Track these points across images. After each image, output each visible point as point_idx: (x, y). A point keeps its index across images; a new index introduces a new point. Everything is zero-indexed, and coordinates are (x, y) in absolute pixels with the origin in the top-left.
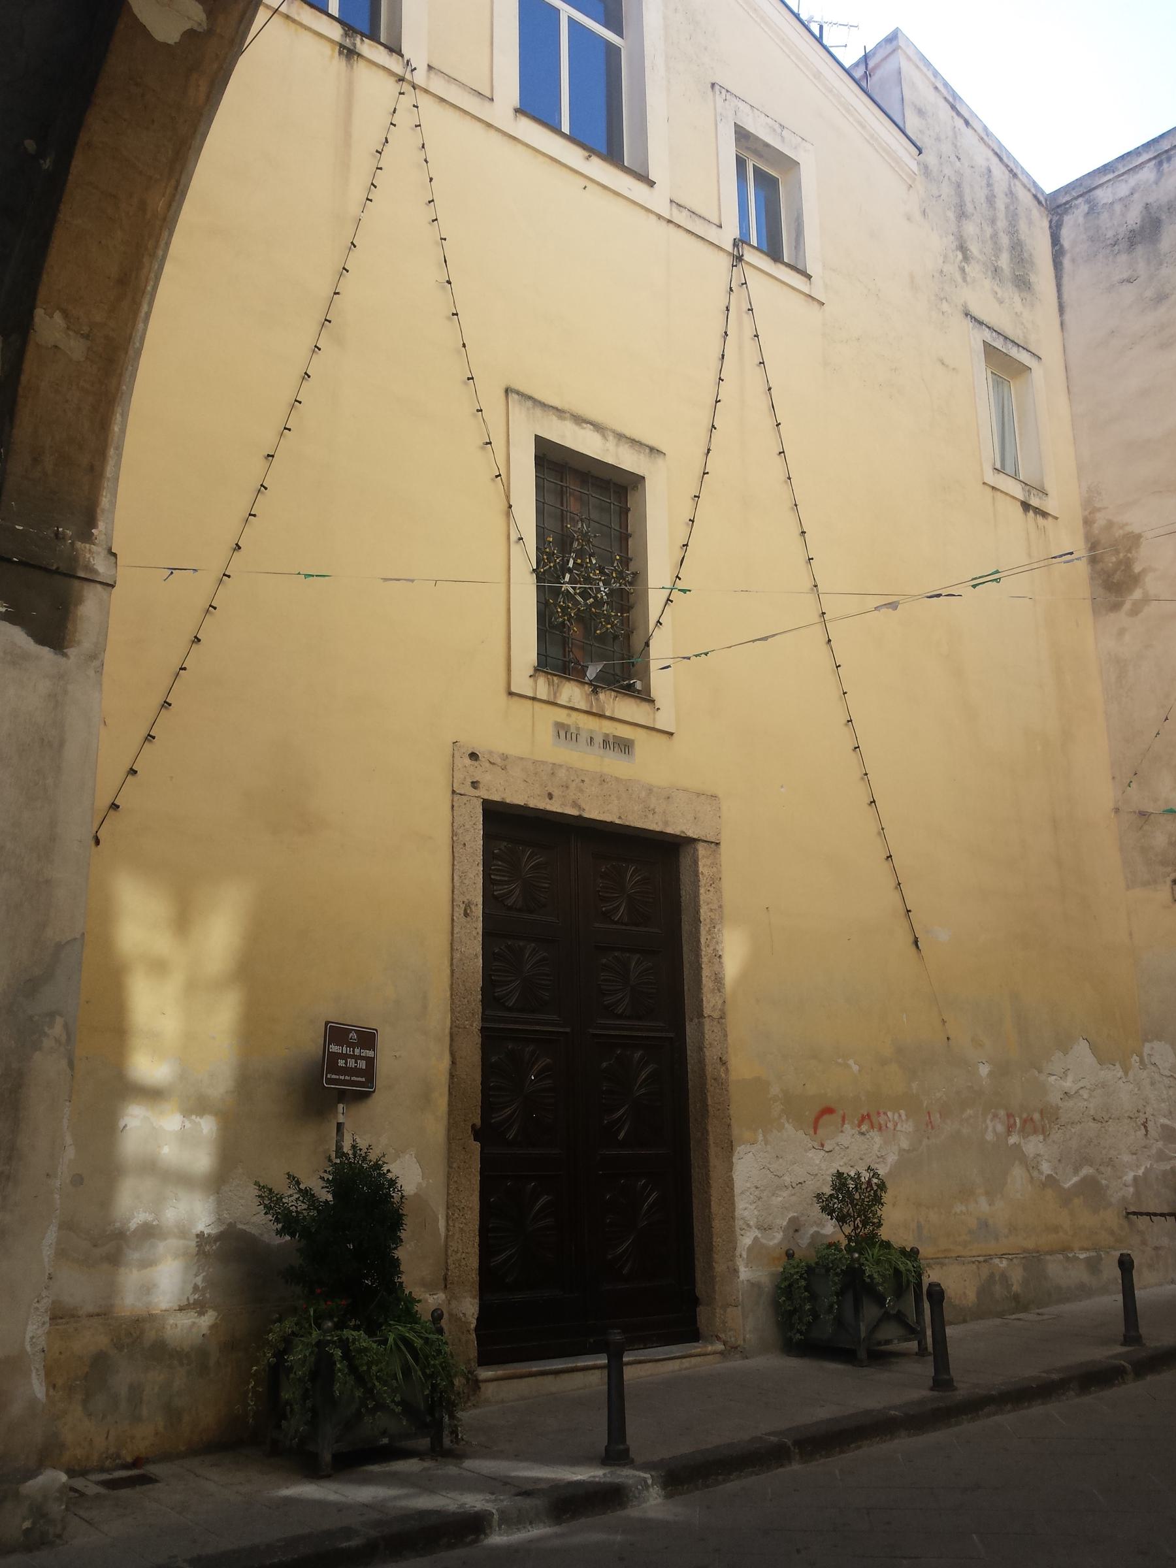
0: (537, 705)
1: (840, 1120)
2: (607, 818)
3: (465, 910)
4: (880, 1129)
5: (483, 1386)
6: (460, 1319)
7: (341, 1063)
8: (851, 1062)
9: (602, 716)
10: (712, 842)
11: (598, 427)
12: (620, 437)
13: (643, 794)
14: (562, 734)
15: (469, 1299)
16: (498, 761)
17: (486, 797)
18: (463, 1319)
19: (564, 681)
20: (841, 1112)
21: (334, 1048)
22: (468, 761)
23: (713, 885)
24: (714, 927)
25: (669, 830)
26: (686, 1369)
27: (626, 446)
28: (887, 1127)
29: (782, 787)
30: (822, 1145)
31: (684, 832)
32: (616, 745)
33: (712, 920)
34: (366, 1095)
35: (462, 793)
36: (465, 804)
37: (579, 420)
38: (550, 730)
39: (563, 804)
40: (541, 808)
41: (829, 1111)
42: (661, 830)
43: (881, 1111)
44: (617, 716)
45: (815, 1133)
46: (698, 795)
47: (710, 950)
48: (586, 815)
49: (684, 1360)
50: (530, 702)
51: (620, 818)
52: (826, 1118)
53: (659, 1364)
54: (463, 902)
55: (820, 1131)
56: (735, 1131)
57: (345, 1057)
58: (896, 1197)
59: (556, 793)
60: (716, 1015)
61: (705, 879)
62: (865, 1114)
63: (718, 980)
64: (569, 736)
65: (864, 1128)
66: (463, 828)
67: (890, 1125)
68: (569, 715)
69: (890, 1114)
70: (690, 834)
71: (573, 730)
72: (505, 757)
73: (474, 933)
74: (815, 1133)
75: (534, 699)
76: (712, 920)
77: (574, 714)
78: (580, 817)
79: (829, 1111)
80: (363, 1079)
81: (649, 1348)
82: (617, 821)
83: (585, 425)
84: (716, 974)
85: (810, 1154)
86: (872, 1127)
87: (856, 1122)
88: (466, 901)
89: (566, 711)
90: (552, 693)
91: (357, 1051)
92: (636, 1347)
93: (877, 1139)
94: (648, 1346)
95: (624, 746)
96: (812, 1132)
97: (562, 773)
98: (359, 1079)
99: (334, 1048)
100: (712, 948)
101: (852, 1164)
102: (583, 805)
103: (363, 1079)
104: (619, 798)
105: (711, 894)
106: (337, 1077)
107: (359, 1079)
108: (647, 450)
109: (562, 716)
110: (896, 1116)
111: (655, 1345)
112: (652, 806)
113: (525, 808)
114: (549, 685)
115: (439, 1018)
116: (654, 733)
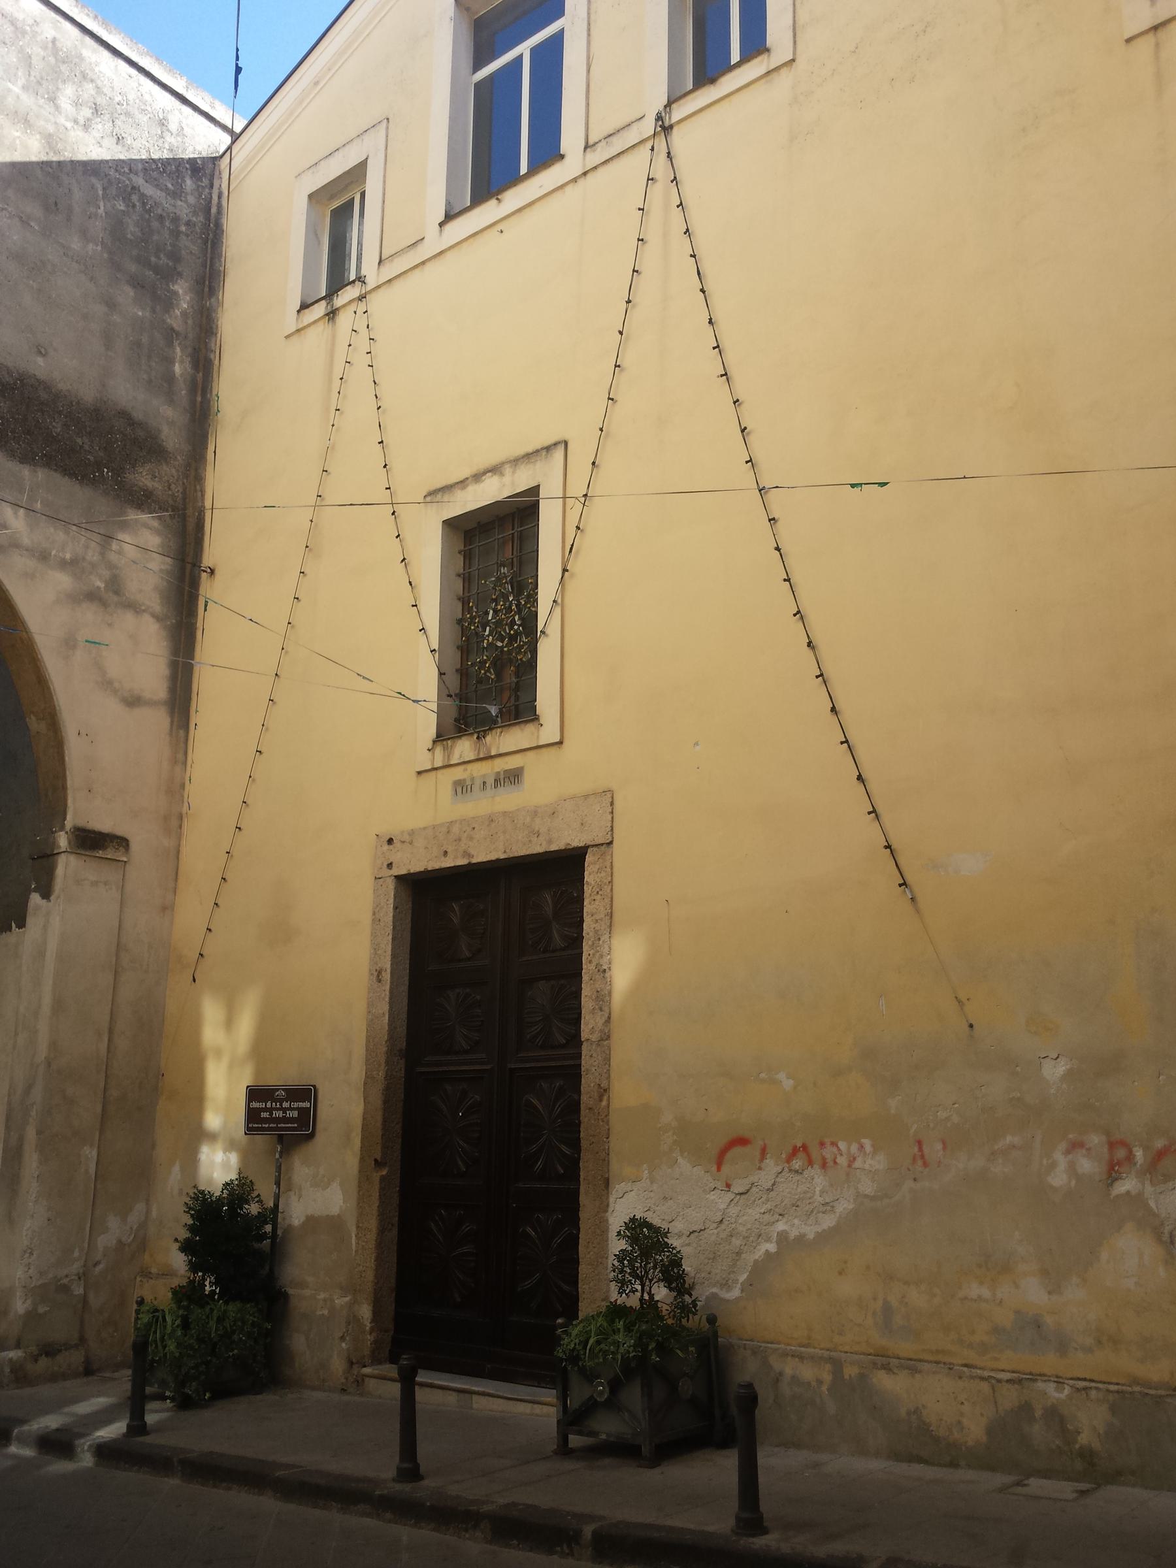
0: (440, 772)
1: (758, 1154)
2: (493, 856)
3: (378, 976)
4: (824, 1165)
5: (367, 1379)
6: (359, 1320)
7: (264, 1115)
8: (782, 1076)
9: (491, 757)
10: (602, 844)
11: (495, 470)
12: (516, 462)
13: (528, 819)
14: (459, 790)
16: (407, 838)
17: (396, 874)
18: (361, 1321)
19: (456, 740)
20: (761, 1143)
21: (255, 1105)
22: (386, 847)
23: (600, 893)
24: (599, 939)
25: (554, 847)
26: (537, 1415)
27: (522, 467)
28: (835, 1162)
29: (696, 744)
30: (728, 1186)
31: (569, 844)
32: (507, 780)
33: (596, 932)
34: (311, 1136)
35: (380, 876)
36: (381, 885)
37: (477, 477)
39: (456, 858)
40: (437, 868)
41: (742, 1141)
42: (544, 851)
43: (827, 1141)
44: (502, 751)
45: (719, 1169)
46: (586, 797)
47: (592, 967)
48: (474, 861)
49: (536, 1406)
50: (434, 773)
51: (505, 852)
52: (737, 1150)
53: (511, 1402)
54: (376, 970)
55: (726, 1169)
56: (615, 1165)
57: (265, 1110)
58: (845, 1262)
60: (594, 1038)
61: (591, 888)
62: (799, 1145)
63: (603, 998)
64: (464, 789)
65: (797, 1164)
66: (379, 906)
67: (842, 1161)
68: (465, 770)
69: (842, 1145)
70: (576, 843)
71: (468, 783)
72: (412, 833)
73: (383, 995)
74: (719, 1169)
75: (436, 769)
76: (596, 932)
77: (469, 767)
78: (470, 864)
79: (742, 1141)
81: (544, 1387)
82: (502, 857)
83: (484, 478)
84: (598, 992)
85: (712, 1196)
86: (811, 1163)
87: (784, 1156)
88: (378, 969)
89: (461, 768)
90: (446, 757)
91: (286, 1105)
92: (525, 1383)
93: (818, 1180)
94: (542, 1385)
95: (514, 777)
96: (714, 1168)
97: (456, 829)
98: (293, 1125)
99: (255, 1105)
100: (594, 963)
101: (781, 1212)
102: (472, 852)
103: (296, 1125)
104: (504, 832)
105: (597, 902)
107: (293, 1125)
108: (544, 453)
109: (458, 773)
110: (854, 1148)
111: (548, 1386)
112: (537, 829)
113: (426, 872)
114: (444, 750)
115: (358, 1072)
116: (544, 750)
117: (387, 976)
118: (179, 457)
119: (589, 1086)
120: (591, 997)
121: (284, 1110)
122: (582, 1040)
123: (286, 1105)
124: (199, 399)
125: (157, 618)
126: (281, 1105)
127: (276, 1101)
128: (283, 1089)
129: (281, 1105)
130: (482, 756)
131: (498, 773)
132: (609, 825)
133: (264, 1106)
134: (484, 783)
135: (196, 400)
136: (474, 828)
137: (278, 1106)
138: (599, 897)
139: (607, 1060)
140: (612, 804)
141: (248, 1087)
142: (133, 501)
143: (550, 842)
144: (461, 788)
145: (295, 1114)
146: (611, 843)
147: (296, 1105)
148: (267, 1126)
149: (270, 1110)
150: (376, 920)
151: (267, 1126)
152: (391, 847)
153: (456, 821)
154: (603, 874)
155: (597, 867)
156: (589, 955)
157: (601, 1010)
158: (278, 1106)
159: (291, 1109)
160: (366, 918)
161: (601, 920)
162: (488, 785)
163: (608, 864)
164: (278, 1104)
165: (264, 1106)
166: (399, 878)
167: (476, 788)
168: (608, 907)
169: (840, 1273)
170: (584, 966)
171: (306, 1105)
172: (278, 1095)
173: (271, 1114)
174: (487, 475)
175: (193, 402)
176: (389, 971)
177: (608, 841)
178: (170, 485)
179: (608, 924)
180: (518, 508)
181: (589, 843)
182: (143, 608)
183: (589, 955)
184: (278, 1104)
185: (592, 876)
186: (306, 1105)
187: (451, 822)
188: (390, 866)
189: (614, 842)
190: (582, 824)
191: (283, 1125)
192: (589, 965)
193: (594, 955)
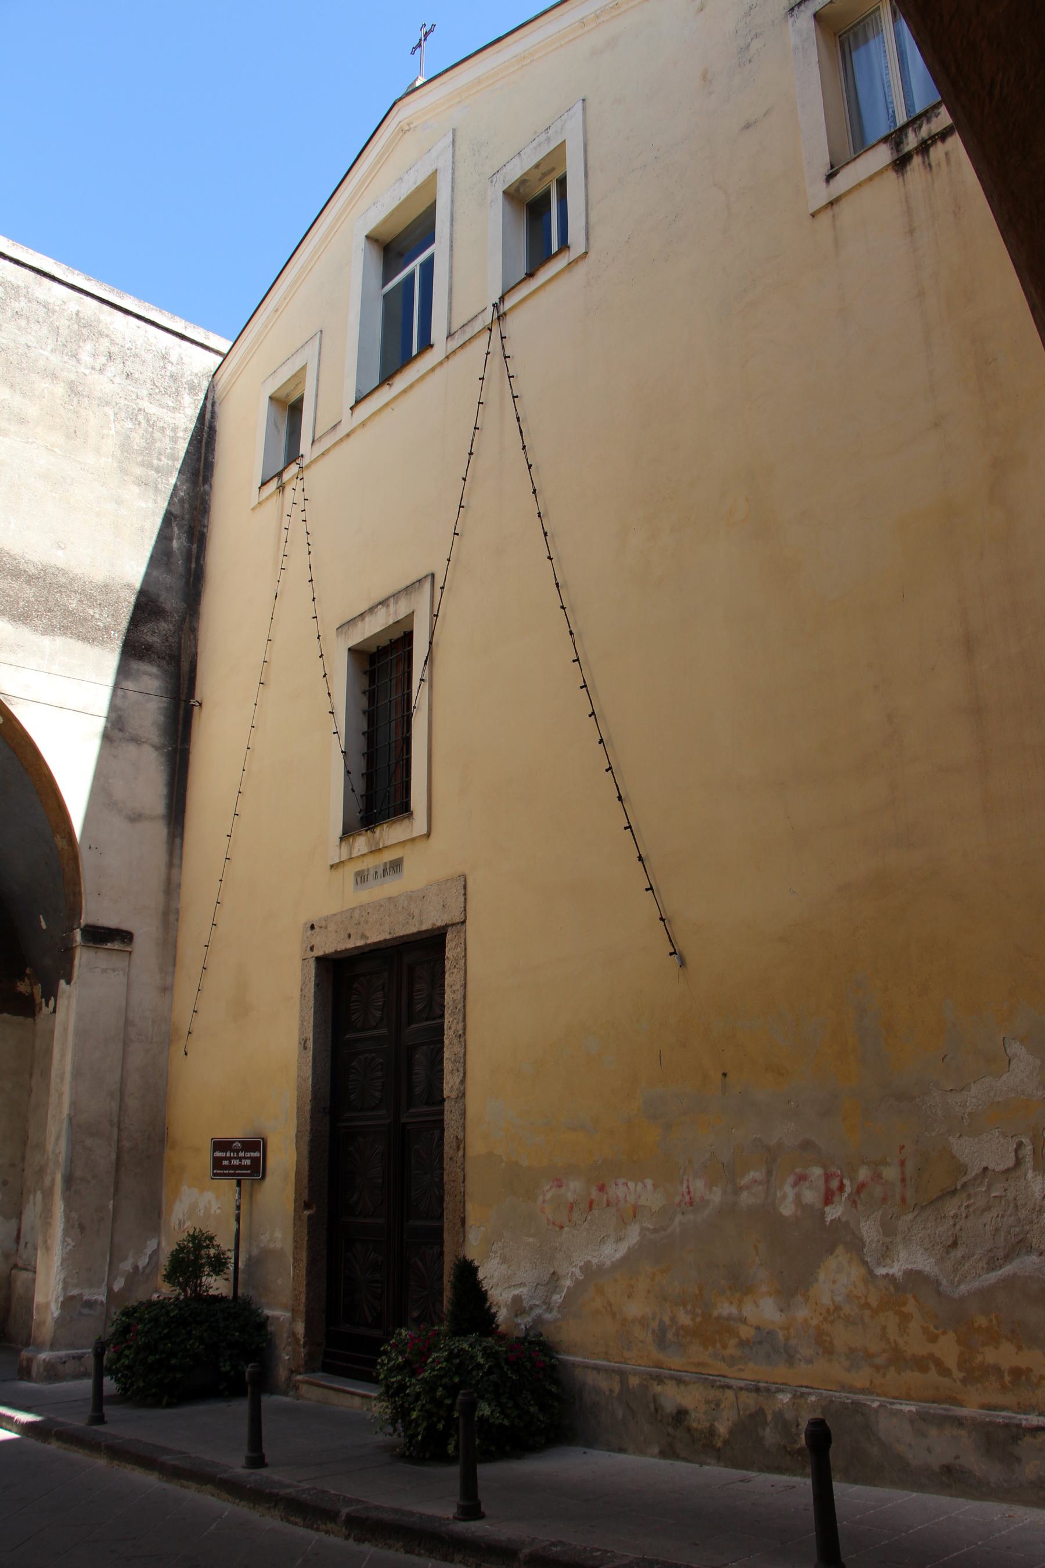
7: (225, 1163)
10: (458, 923)
14: (359, 880)
15: (300, 1323)
16: (323, 924)
21: (218, 1154)
22: (309, 932)
23: (457, 966)
25: (424, 928)
32: (391, 868)
35: (305, 958)
38: (351, 880)
48: (369, 941)
51: (390, 933)
57: (225, 1158)
59: (352, 932)
60: (453, 1095)
69: (631, 1185)
70: (439, 924)
73: (308, 1061)
80: (249, 1172)
82: (388, 937)
84: (455, 1054)
91: (241, 1154)
99: (218, 1154)
103: (249, 1172)
106: (222, 1172)
117: (310, 1044)
118: (175, 615)
119: (450, 1138)
120: (450, 1059)
121: (240, 1159)
122: (445, 1097)
123: (241, 1154)
124: (193, 566)
125: (156, 748)
126: (238, 1154)
127: (234, 1151)
128: (239, 1142)
129: (238, 1154)
130: (373, 849)
131: (386, 863)
132: (463, 906)
133: (224, 1155)
134: (376, 872)
135: (190, 566)
136: (369, 913)
137: (235, 1155)
138: (455, 970)
139: (463, 1114)
140: (465, 887)
141: (212, 1139)
142: (136, 655)
143: (421, 922)
144: (361, 877)
145: (248, 1162)
146: (464, 922)
147: (248, 1155)
148: (227, 1172)
149: (230, 1159)
150: (303, 996)
151: (227, 1172)
152: (313, 932)
153: (357, 907)
154: (459, 950)
155: (454, 943)
156: (449, 1022)
157: (458, 1071)
158: (235, 1155)
159: (245, 1158)
160: (297, 994)
161: (458, 990)
162: (379, 874)
163: (463, 942)
164: (235, 1153)
165: (224, 1155)
166: (319, 960)
167: (370, 878)
168: (462, 979)
169: (629, 1297)
170: (446, 1032)
171: (257, 1154)
172: (235, 1147)
173: (230, 1162)
174: (379, 607)
175: (188, 569)
176: (312, 1039)
177: (462, 920)
178: (167, 637)
179: (463, 994)
180: (405, 632)
181: (448, 922)
182: (144, 740)
183: (449, 1022)
184: (235, 1153)
185: (450, 952)
186: (257, 1154)
187: (354, 908)
188: (312, 949)
189: (467, 921)
190: (444, 906)
191: (240, 1172)
192: (449, 1031)
193: (452, 1021)
